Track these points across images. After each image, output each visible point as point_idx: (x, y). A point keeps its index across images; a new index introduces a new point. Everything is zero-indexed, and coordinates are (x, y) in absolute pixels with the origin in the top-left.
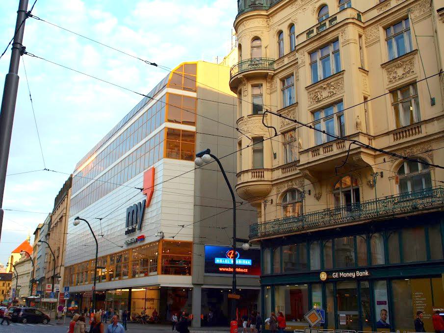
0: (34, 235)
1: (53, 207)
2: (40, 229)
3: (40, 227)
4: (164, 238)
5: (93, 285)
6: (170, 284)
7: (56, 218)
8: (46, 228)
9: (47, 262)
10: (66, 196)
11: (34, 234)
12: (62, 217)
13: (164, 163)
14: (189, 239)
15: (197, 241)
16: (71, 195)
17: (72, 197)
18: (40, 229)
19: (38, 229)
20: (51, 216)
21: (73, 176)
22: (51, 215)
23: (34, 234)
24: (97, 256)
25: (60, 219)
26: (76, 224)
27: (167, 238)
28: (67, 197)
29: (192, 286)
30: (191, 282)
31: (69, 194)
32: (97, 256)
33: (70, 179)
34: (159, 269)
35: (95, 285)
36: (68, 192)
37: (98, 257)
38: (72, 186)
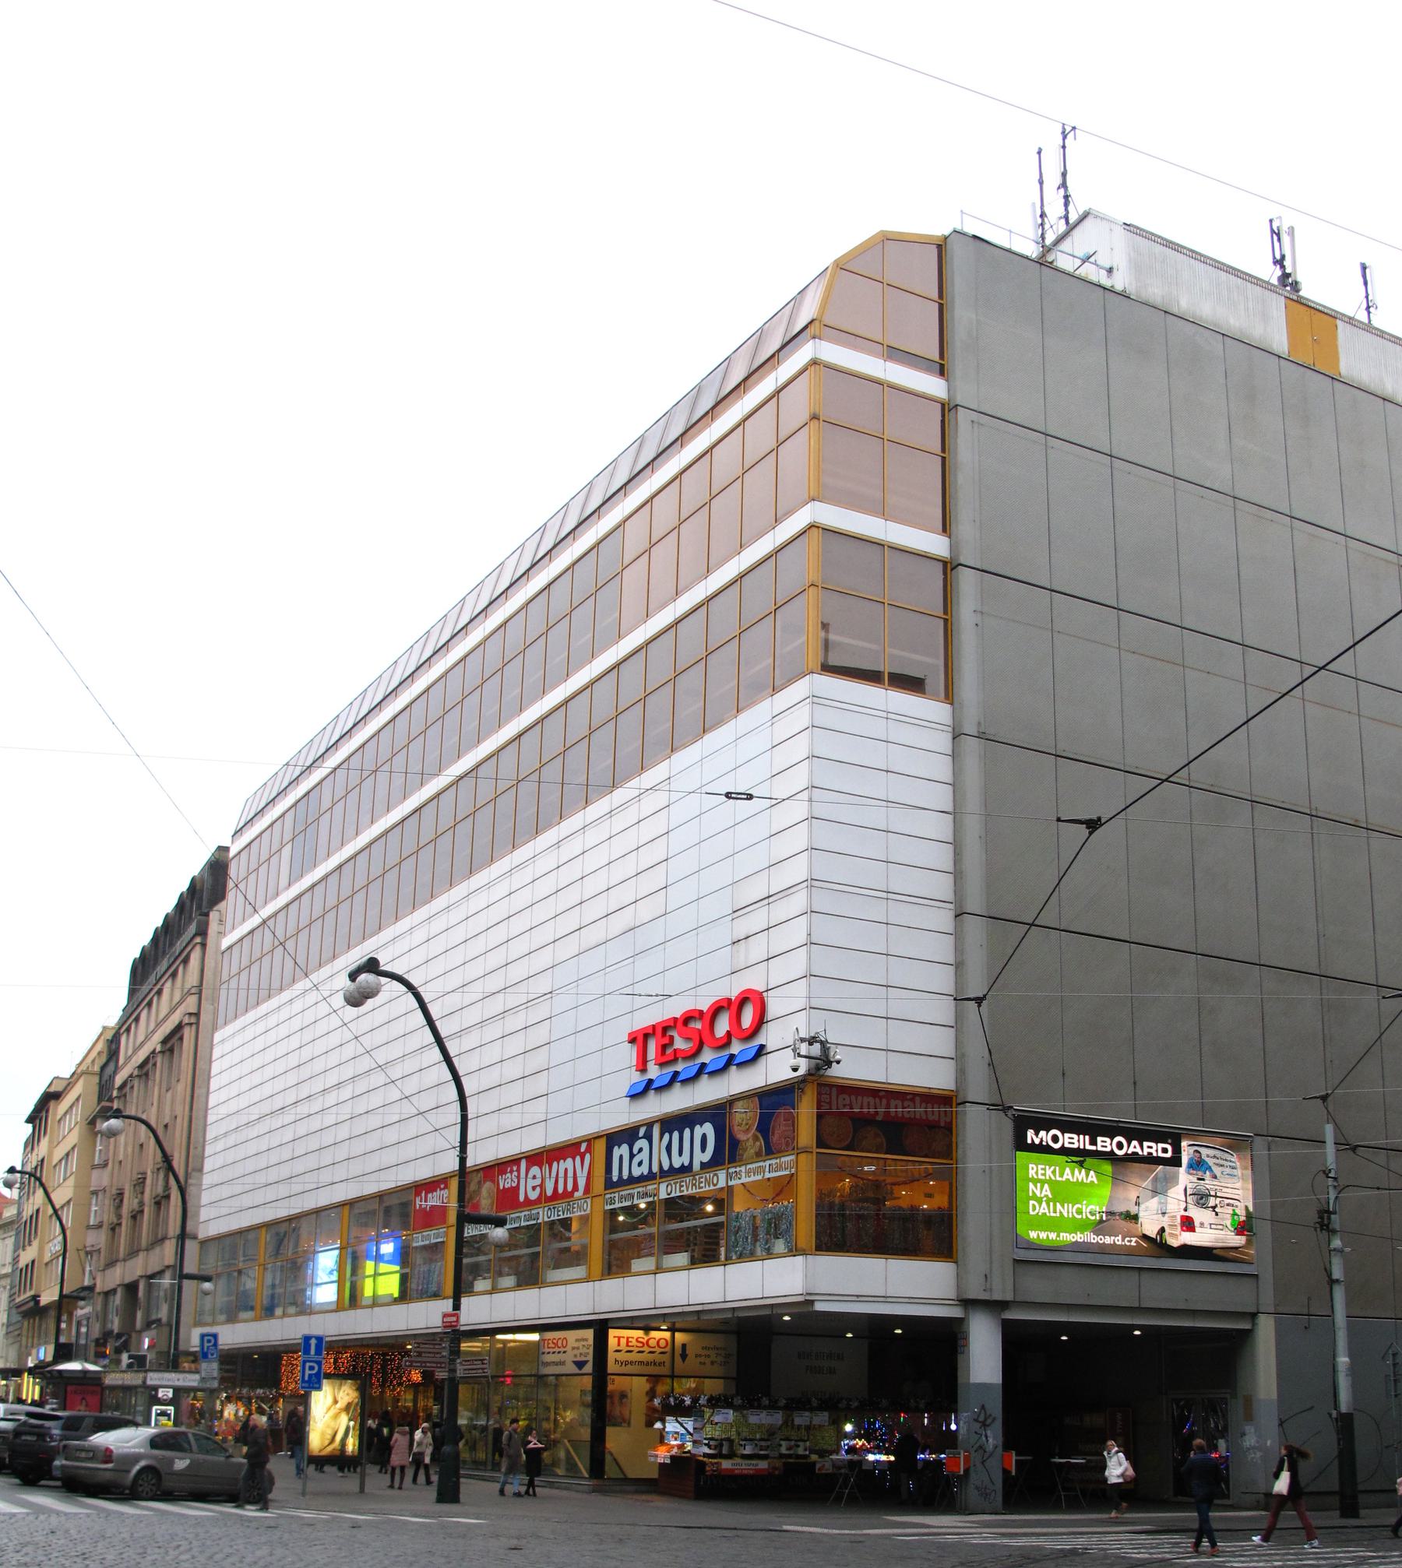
0: (30, 1126)
1: (121, 998)
3: (57, 1087)
4: (836, 1072)
5: (447, 1305)
6: (859, 1298)
7: (145, 1040)
9: (99, 1226)
10: (198, 940)
12: (179, 1027)
13: (814, 699)
14: (936, 1077)
15: (978, 1088)
16: (222, 934)
17: (226, 942)
19: (50, 1098)
20: (112, 1044)
21: (232, 853)
22: (109, 1035)
24: (463, 1160)
25: (164, 1042)
26: (356, 1000)
27: (849, 1068)
28: (204, 945)
29: (955, 1312)
30: (951, 1293)
31: (213, 927)
32: (463, 1160)
33: (218, 868)
34: (805, 1227)
35: (457, 1306)
36: (207, 924)
37: (469, 1163)
38: (231, 895)
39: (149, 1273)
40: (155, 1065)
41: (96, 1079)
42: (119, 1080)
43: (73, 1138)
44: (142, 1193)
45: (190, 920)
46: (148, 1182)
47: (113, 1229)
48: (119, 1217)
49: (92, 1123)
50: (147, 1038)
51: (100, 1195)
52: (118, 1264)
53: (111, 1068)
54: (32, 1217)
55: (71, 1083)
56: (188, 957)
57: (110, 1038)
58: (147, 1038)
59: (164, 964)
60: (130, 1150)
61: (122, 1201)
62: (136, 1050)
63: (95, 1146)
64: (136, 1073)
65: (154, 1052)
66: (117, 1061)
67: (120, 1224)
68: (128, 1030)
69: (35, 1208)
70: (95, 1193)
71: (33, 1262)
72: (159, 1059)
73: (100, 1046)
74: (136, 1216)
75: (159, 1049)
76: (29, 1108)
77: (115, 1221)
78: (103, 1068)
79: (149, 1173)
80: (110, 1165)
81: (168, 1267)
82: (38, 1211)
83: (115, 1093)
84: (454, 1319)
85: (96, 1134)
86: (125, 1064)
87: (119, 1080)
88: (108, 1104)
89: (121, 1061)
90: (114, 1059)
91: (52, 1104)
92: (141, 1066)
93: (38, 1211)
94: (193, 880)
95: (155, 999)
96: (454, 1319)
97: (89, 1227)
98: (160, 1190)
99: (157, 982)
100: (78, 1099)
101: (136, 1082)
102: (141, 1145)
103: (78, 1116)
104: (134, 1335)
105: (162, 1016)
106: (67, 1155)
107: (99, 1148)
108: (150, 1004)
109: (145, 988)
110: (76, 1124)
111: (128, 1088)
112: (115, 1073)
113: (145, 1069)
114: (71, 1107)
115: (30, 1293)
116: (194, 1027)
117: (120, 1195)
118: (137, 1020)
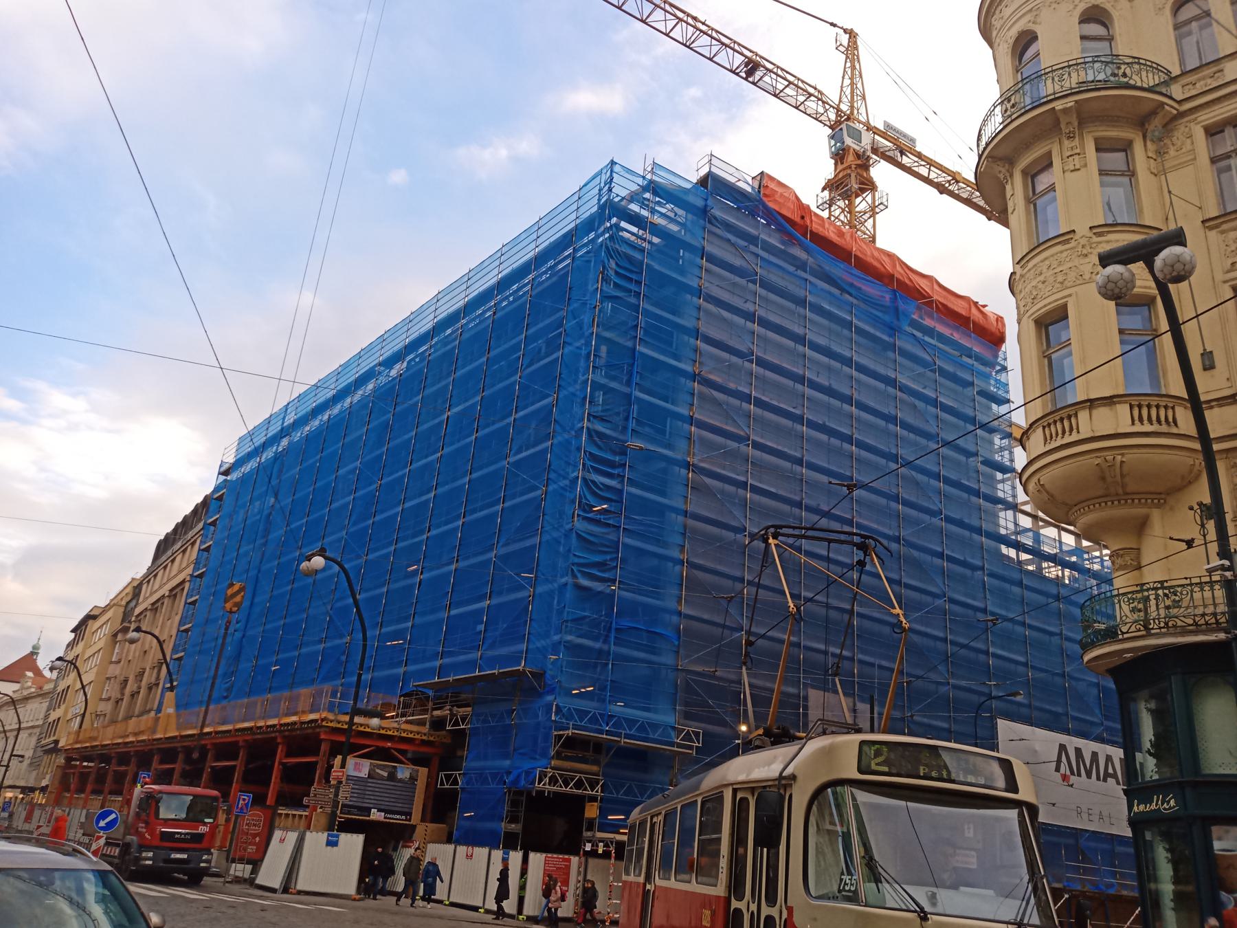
0: (73, 635)
1: (149, 562)
2: (94, 617)
3: (95, 612)
8: (116, 614)
9: (109, 699)
11: (72, 631)
12: (183, 582)
18: (94, 617)
19: (90, 618)
20: (136, 589)
22: (135, 584)
23: (72, 631)
25: (171, 591)
40: (163, 603)
41: (122, 609)
43: (101, 644)
44: (141, 681)
45: (200, 520)
46: (146, 674)
47: (117, 702)
48: (123, 694)
49: (115, 635)
50: (160, 587)
51: (112, 680)
53: (133, 603)
55: (105, 610)
56: (195, 541)
57: (135, 585)
58: (160, 587)
59: (179, 544)
60: (137, 654)
61: (126, 685)
62: (151, 594)
63: (115, 647)
65: (163, 596)
66: (138, 600)
67: (122, 699)
68: (149, 582)
70: (109, 679)
71: (59, 719)
72: (166, 601)
73: (129, 590)
74: (134, 695)
75: (167, 594)
76: (75, 623)
77: (119, 696)
78: (128, 603)
79: (148, 669)
80: (122, 663)
82: (68, 687)
83: (133, 619)
84: (340, 774)
85: (116, 643)
86: (143, 601)
87: (137, 611)
89: (141, 600)
90: (136, 598)
91: (90, 622)
92: (153, 604)
93: (68, 687)
94: (206, 496)
95: (170, 564)
96: (340, 774)
98: (153, 680)
99: (173, 554)
100: (108, 621)
101: (148, 613)
102: (145, 652)
103: (106, 630)
105: (172, 575)
107: (116, 651)
108: (165, 567)
109: (164, 558)
110: (104, 635)
111: (142, 616)
112: (135, 606)
113: (155, 607)
114: (103, 625)
115: (52, 738)
117: (126, 681)
118: (155, 576)
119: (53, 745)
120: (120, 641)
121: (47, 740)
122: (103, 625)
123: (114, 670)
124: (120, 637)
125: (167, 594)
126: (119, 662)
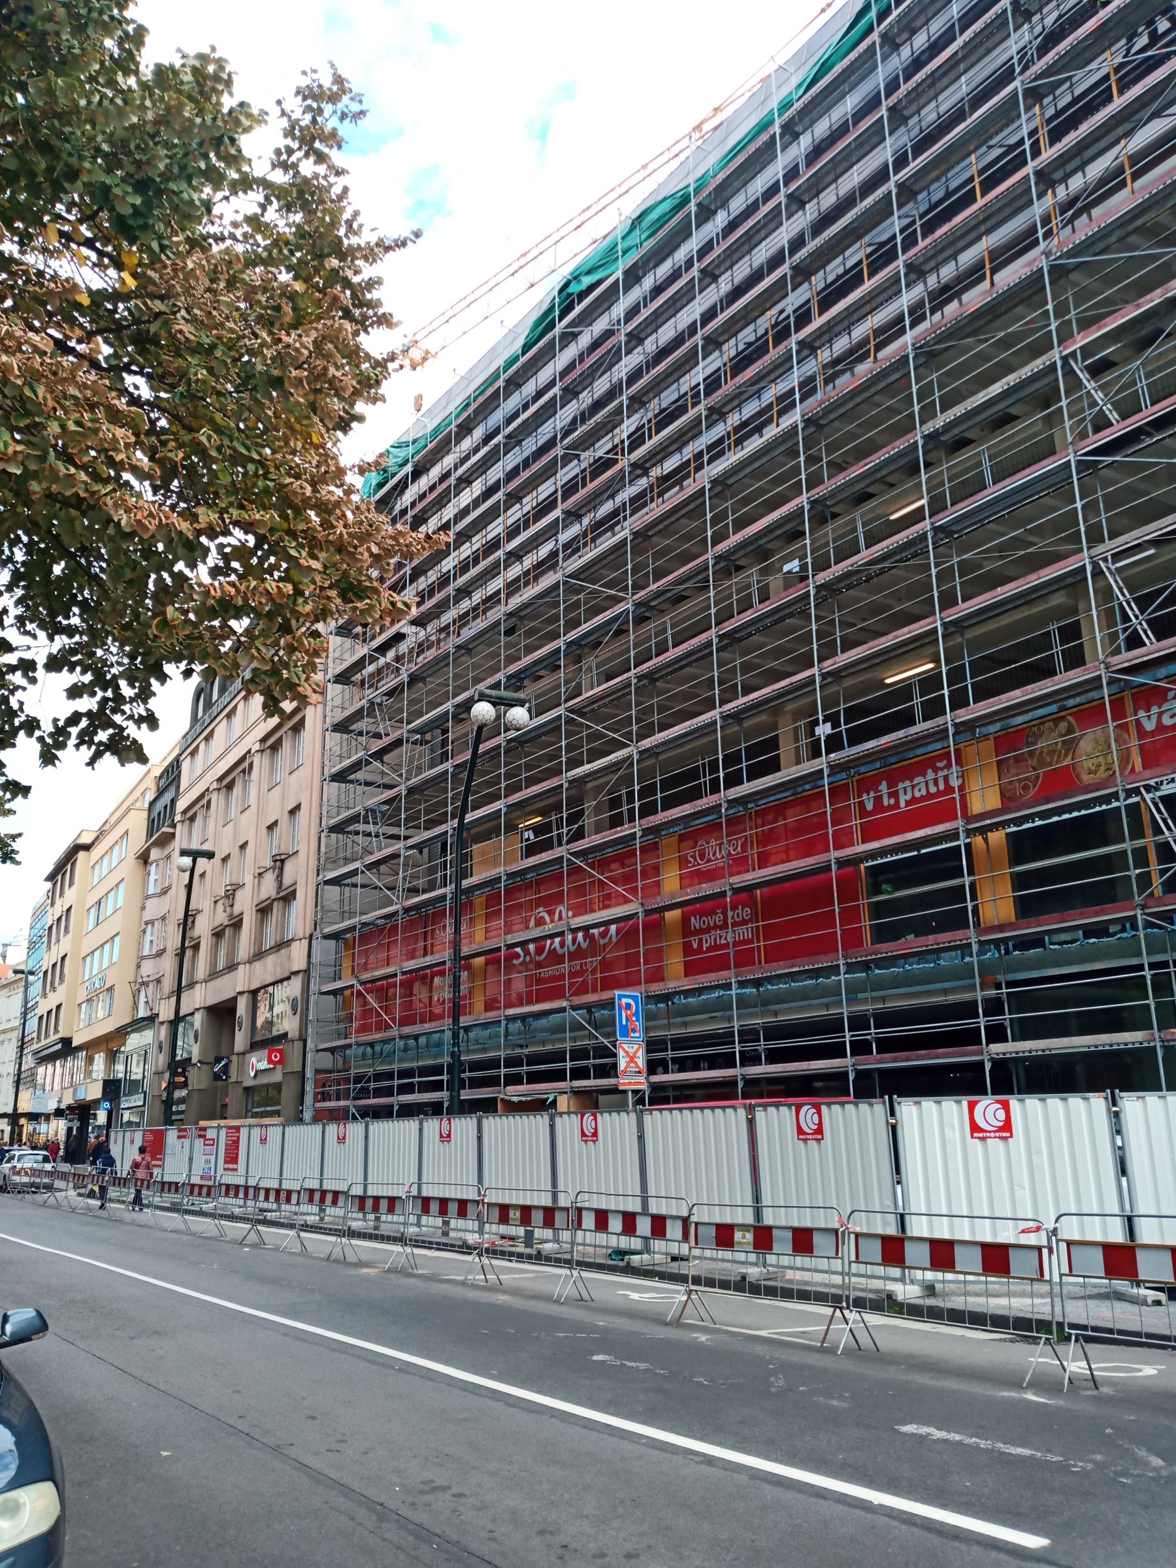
0: (49, 885)
2: (87, 848)
3: (86, 839)
8: (137, 822)
9: (160, 953)
18: (87, 848)
25: (263, 740)
39: (254, 986)
41: (145, 814)
42: (181, 805)
50: (241, 737)
52: (198, 986)
53: (159, 806)
54: (54, 965)
64: (215, 785)
65: (249, 751)
66: (178, 788)
69: (61, 954)
71: (59, 1007)
72: (257, 760)
76: (50, 868)
78: (152, 804)
81: (296, 973)
82: (63, 958)
83: (178, 818)
86: (192, 785)
87: (181, 805)
88: (171, 830)
91: (81, 855)
93: (63, 958)
95: (241, 706)
97: (143, 958)
98: (268, 887)
104: (234, 1058)
106: (99, 903)
107: (153, 877)
114: (111, 848)
115: (53, 1038)
116: (320, 707)
119: (59, 1046)
120: (156, 861)
121: (43, 1042)
122: (111, 848)
123: (154, 909)
124: (155, 854)
125: (257, 747)
126: (164, 892)
